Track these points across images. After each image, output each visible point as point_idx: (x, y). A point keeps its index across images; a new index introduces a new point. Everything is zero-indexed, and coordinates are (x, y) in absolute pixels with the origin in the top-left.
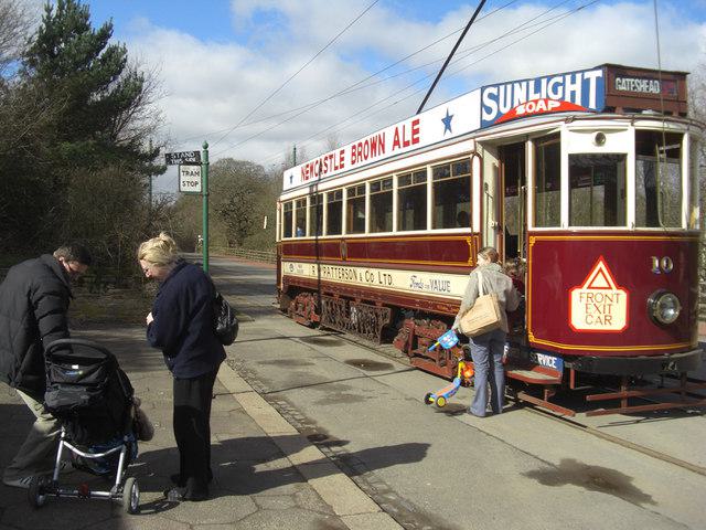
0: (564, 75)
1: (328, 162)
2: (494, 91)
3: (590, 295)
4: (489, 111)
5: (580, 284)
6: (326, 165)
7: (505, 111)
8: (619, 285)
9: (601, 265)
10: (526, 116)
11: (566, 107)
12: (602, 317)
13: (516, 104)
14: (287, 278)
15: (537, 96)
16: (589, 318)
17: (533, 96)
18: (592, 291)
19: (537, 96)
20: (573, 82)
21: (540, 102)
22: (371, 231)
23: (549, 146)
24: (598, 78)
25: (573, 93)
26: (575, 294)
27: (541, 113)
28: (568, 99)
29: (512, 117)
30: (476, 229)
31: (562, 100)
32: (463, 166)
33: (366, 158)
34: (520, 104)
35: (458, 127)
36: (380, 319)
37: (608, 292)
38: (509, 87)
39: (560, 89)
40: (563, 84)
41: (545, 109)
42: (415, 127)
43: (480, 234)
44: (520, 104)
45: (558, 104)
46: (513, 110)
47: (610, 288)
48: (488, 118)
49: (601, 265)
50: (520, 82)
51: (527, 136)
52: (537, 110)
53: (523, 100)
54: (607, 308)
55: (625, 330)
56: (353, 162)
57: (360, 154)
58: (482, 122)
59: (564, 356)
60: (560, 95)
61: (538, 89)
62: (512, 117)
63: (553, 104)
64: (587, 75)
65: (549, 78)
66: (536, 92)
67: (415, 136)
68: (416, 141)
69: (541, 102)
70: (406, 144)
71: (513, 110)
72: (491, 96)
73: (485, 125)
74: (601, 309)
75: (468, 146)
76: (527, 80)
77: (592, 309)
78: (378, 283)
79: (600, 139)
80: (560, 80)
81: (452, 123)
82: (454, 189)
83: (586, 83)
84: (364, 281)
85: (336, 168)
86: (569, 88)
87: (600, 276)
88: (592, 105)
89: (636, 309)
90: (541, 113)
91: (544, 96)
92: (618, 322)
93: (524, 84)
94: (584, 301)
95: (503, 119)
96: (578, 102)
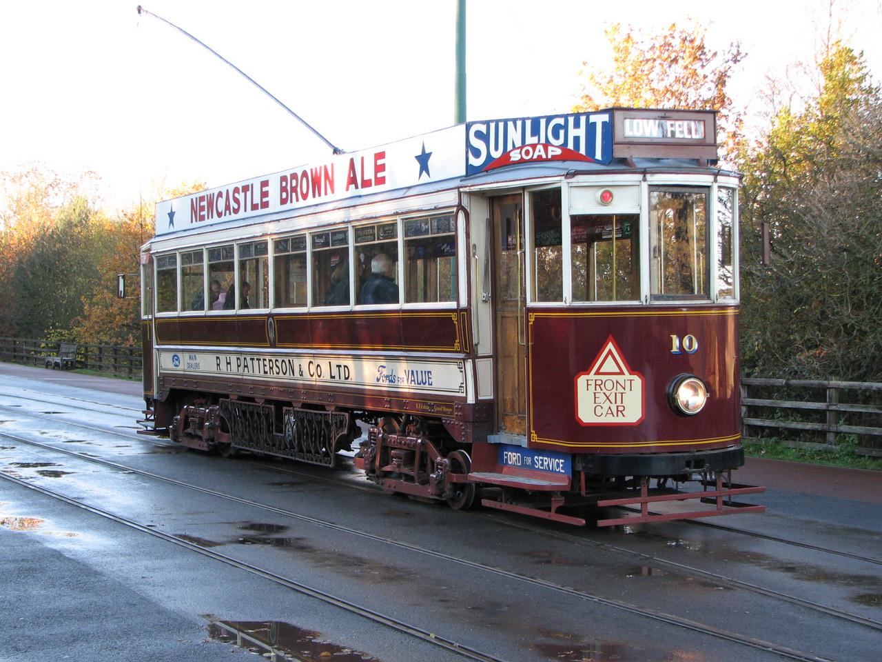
0: (566, 117)
1: (241, 196)
2: (483, 129)
4: (477, 153)
5: (586, 369)
6: (237, 201)
7: (496, 155)
8: (634, 368)
9: (610, 346)
11: (568, 155)
13: (510, 148)
14: (164, 378)
15: (534, 140)
16: (598, 408)
17: (530, 140)
18: (604, 378)
19: (534, 140)
20: (577, 125)
21: (540, 147)
22: (315, 304)
23: (548, 202)
24: (604, 123)
25: (577, 139)
26: (582, 381)
27: (540, 159)
28: (571, 146)
29: (504, 163)
30: (463, 303)
31: (564, 146)
32: (444, 219)
33: (305, 197)
34: (514, 148)
36: (333, 428)
37: (620, 378)
38: (501, 125)
39: (562, 132)
40: (566, 127)
42: (380, 162)
43: (468, 310)
44: (514, 148)
45: (559, 152)
46: (506, 155)
47: (622, 373)
48: (476, 162)
49: (610, 346)
50: (514, 121)
51: (524, 188)
53: (518, 144)
54: (619, 396)
55: (641, 422)
56: (283, 202)
57: (294, 189)
58: (469, 168)
59: (573, 456)
60: (561, 141)
61: (535, 131)
62: (504, 163)
64: (593, 119)
65: (549, 119)
66: (533, 134)
67: (380, 175)
68: (381, 181)
69: (540, 147)
70: (366, 184)
71: (506, 155)
72: (479, 135)
73: (471, 171)
74: (612, 398)
75: (450, 198)
76: (524, 120)
77: (601, 398)
78: (328, 377)
79: (606, 198)
80: (561, 121)
81: (430, 163)
82: (432, 245)
83: (591, 128)
84: (306, 375)
85: (254, 207)
86: (573, 132)
87: (610, 360)
88: (598, 156)
91: (543, 141)
92: (632, 411)
93: (519, 123)
94: (592, 388)
95: (492, 166)
96: (582, 151)
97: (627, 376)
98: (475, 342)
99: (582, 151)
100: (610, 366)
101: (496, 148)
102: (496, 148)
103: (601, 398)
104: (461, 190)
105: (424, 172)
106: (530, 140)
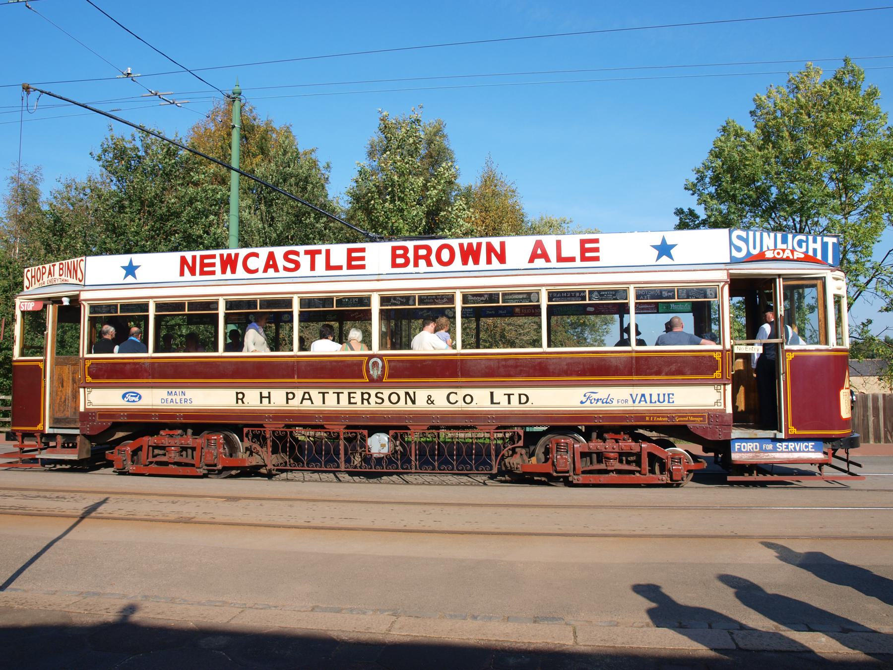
4: (739, 249)
7: (755, 252)
10: (774, 259)
13: (765, 249)
15: (784, 247)
17: (780, 245)
19: (784, 247)
20: (815, 241)
25: (815, 250)
27: (788, 259)
28: (811, 253)
29: (761, 258)
31: (806, 253)
39: (804, 245)
40: (807, 241)
41: (791, 257)
44: (768, 249)
45: (802, 256)
46: (762, 254)
52: (785, 257)
53: (772, 247)
60: (804, 249)
62: (761, 258)
63: (797, 255)
71: (762, 254)
73: (734, 261)
86: (812, 246)
88: (830, 261)
90: (788, 259)
95: (751, 259)
96: (819, 257)
99: (819, 257)
101: (754, 248)
102: (754, 248)
106: (780, 245)
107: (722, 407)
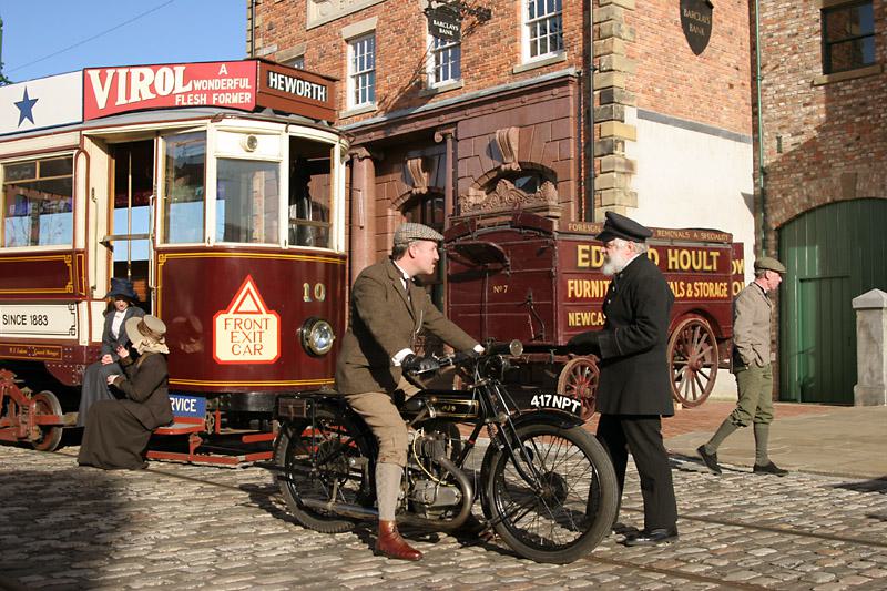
3: (238, 322)
5: (225, 307)
8: (270, 307)
9: (249, 285)
12: (251, 346)
18: (244, 317)
26: (220, 320)
35: (41, 116)
37: (258, 317)
47: (260, 312)
49: (249, 285)
54: (258, 335)
74: (251, 337)
77: (240, 337)
87: (249, 298)
89: (290, 340)
92: (270, 351)
94: (231, 327)
97: (265, 315)
98: (92, 284)
100: (248, 305)
103: (240, 337)
104: (84, 132)
105: (26, 119)
107: (76, 337)
